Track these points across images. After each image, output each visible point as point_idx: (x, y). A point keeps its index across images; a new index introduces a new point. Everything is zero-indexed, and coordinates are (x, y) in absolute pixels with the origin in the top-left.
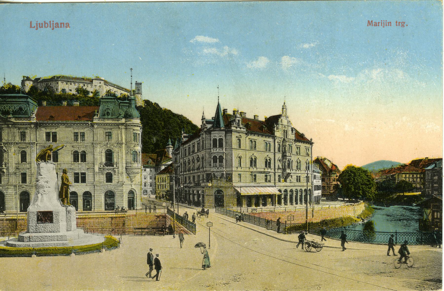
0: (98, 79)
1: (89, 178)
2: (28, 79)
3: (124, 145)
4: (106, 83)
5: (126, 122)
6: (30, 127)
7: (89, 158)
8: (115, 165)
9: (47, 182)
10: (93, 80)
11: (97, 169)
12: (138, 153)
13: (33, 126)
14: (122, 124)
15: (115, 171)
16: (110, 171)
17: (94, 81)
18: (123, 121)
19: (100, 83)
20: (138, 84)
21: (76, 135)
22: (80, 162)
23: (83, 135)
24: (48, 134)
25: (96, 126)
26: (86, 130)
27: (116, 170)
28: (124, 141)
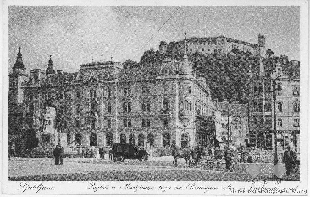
0: (221, 37)
1: (152, 124)
3: (177, 96)
4: (229, 40)
5: (179, 77)
9: (49, 118)
10: (216, 38)
12: (189, 101)
14: (176, 79)
15: (170, 118)
17: (217, 39)
18: (177, 76)
19: (223, 40)
20: (261, 38)
25: (157, 82)
27: (171, 116)
28: (177, 92)
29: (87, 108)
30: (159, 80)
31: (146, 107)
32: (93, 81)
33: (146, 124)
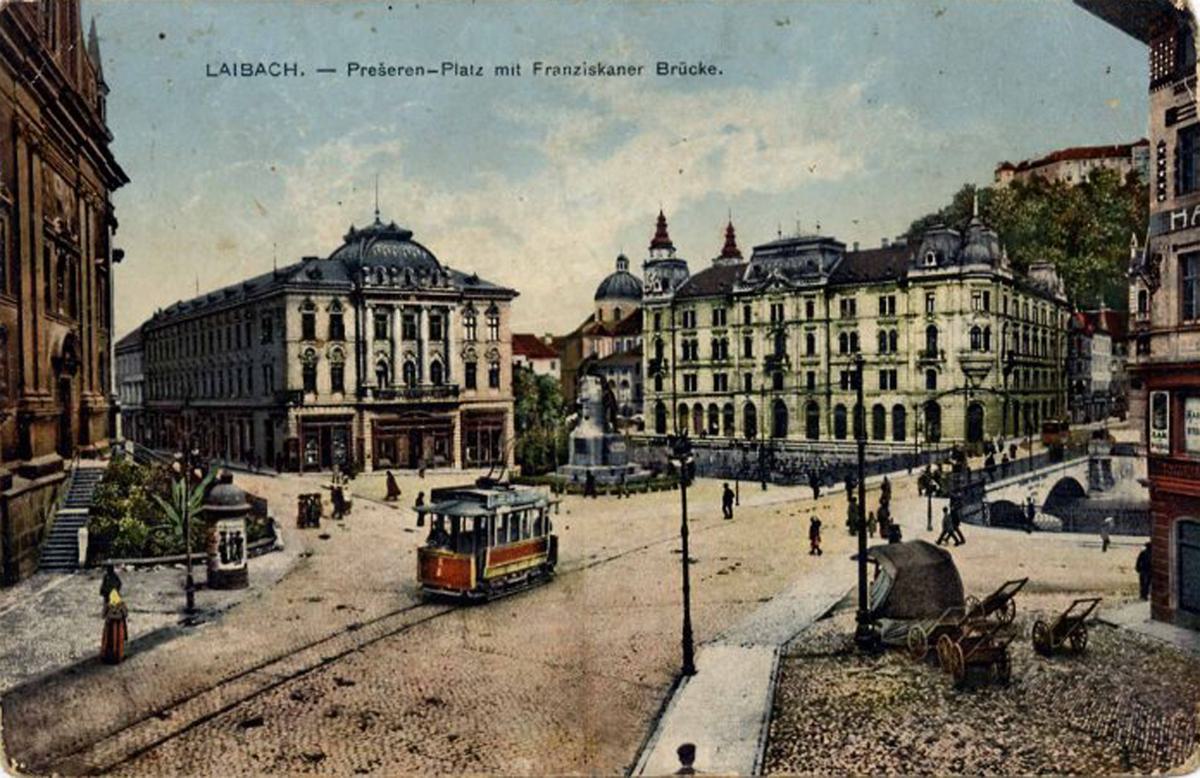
1: (901, 381)
2: (1006, 167)
6: (820, 295)
7: (902, 344)
8: (939, 357)
11: (912, 365)
12: (982, 330)
13: (822, 291)
15: (939, 368)
16: (932, 368)
21: (882, 301)
22: (888, 351)
23: (892, 300)
24: (843, 303)
25: (910, 284)
26: (898, 293)
29: (763, 347)
30: (915, 280)
31: (888, 342)
32: (777, 286)
33: (888, 381)
